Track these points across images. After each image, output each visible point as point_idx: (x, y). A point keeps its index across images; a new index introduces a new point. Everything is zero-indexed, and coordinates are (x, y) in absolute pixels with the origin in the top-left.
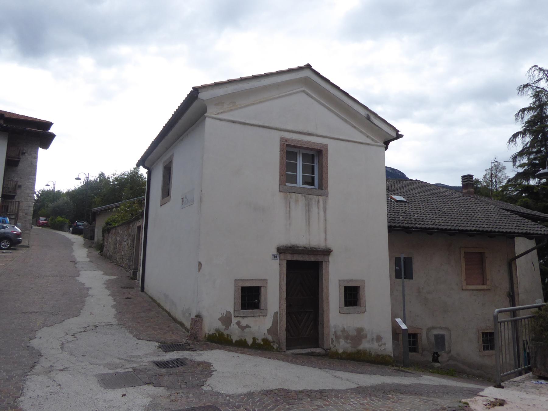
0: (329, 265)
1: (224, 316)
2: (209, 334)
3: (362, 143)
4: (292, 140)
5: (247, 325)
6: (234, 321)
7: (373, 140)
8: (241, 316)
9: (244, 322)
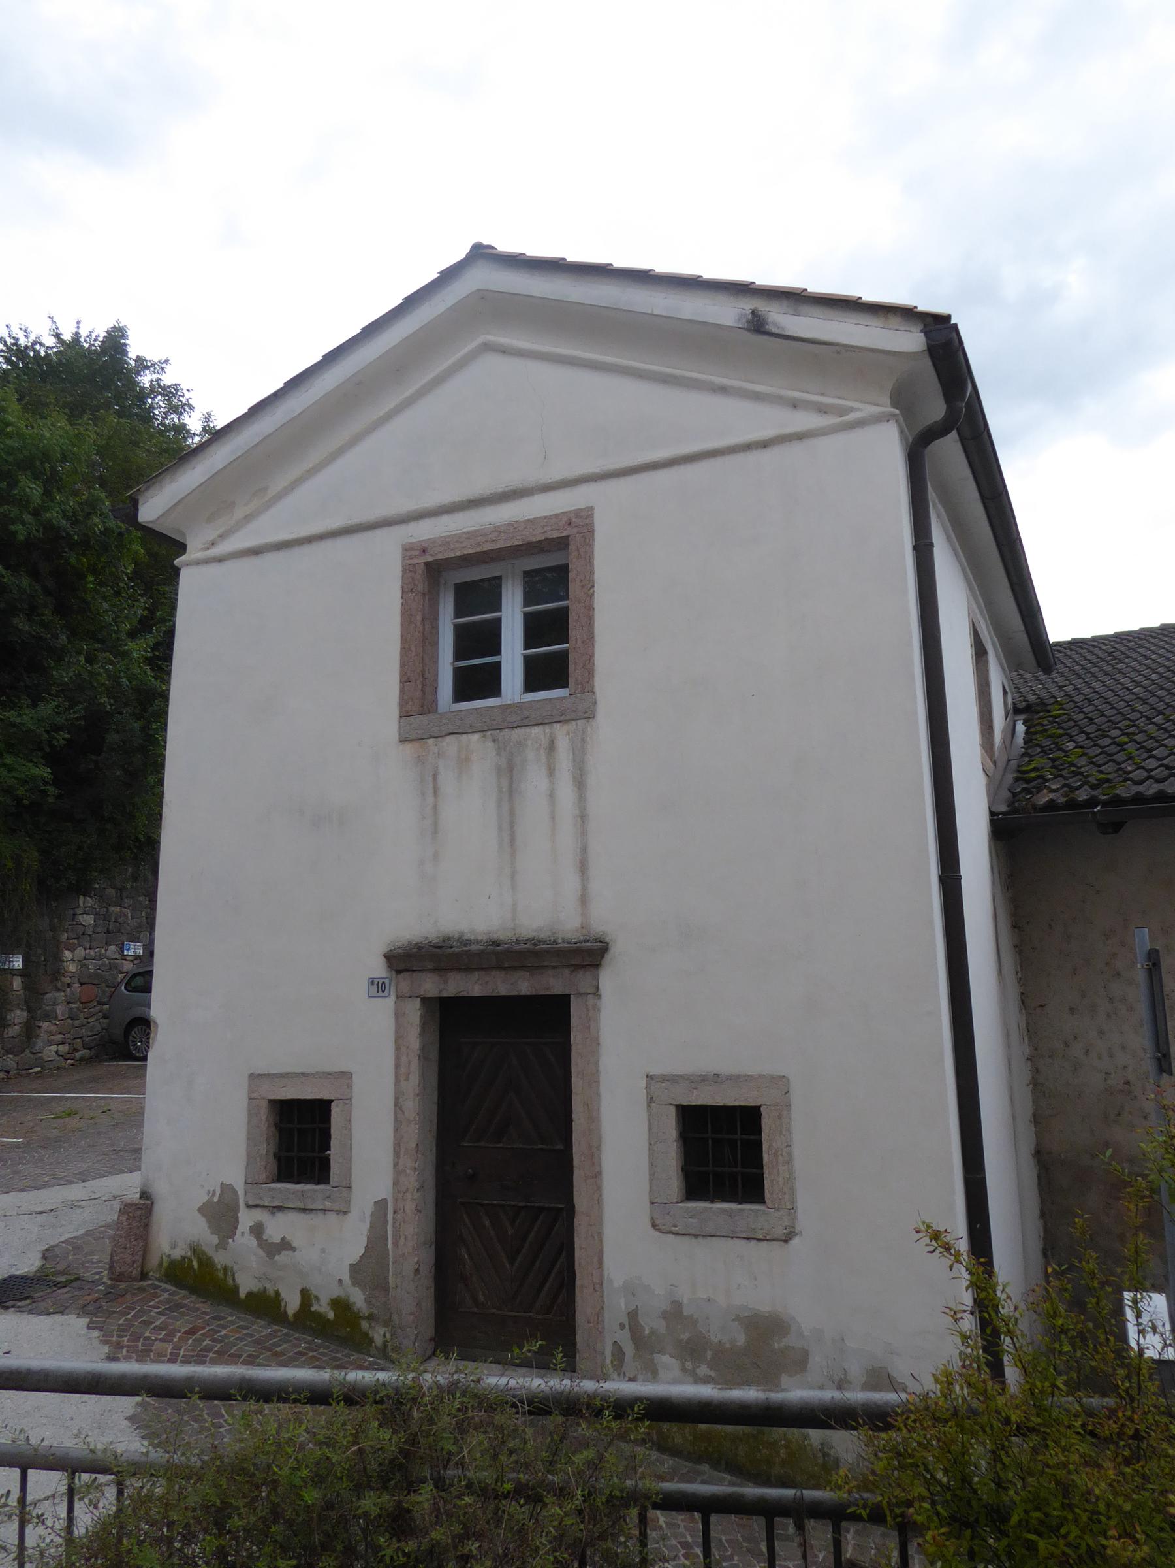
0: (597, 1009)
1: (216, 1199)
2: (173, 1257)
3: (764, 444)
4: (446, 542)
5: (283, 1239)
6: (247, 1219)
7: (822, 409)
8: (264, 1207)
9: (277, 1227)
